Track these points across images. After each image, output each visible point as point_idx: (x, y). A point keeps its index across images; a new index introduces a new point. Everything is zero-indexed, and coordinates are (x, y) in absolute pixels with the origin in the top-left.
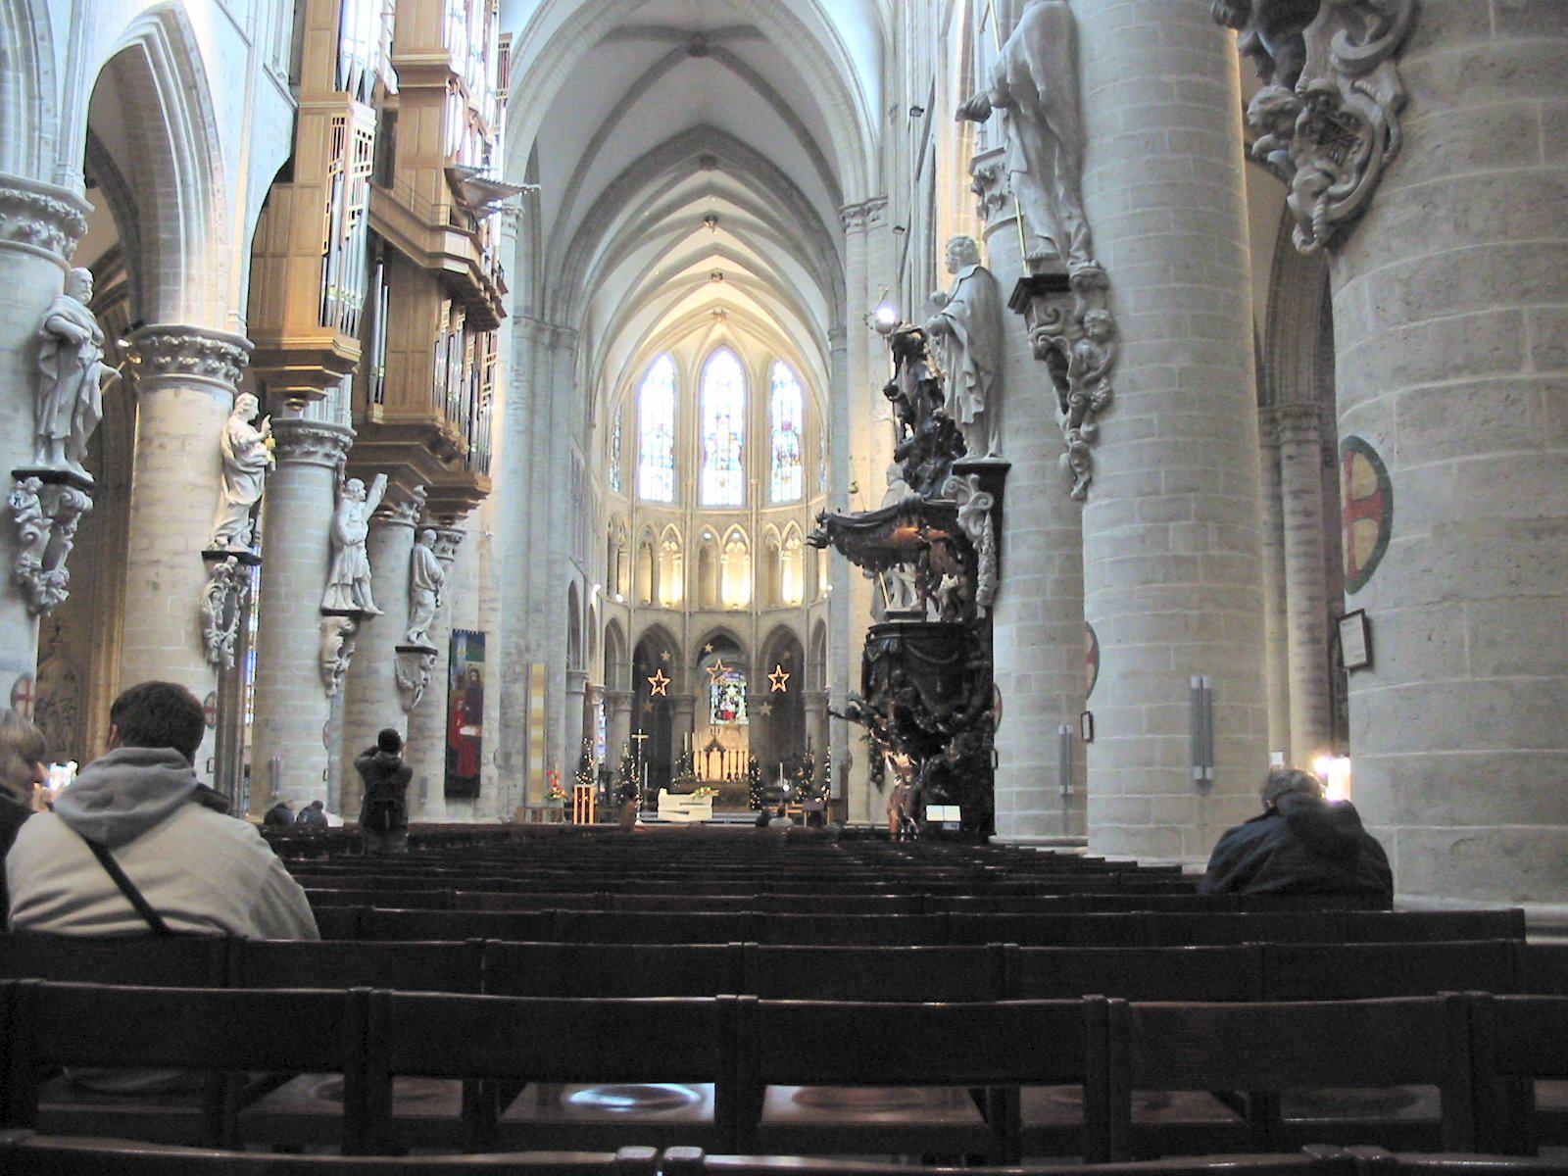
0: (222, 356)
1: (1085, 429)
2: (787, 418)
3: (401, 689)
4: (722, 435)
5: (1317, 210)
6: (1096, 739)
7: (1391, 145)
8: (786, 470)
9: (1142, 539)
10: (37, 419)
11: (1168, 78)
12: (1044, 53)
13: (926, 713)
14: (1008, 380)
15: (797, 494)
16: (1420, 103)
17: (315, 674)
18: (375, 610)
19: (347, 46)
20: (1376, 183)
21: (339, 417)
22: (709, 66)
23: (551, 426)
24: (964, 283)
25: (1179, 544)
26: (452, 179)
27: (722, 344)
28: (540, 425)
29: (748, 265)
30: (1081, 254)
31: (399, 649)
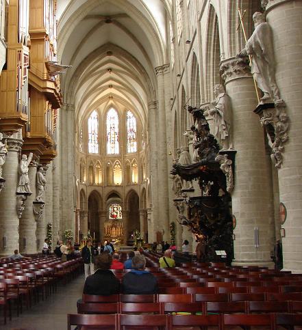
1: (280, 147)
2: (132, 128)
3: (35, 214)
4: (112, 132)
6: (286, 236)
8: (132, 143)
9: (300, 179)
12: (263, 39)
13: (209, 223)
14: (235, 127)
15: (135, 151)
19: (21, 30)
21: (19, 136)
22: (112, 26)
23: (67, 133)
26: (47, 65)
27: (112, 106)
28: (64, 133)
29: (120, 83)
30: (277, 97)
31: (34, 203)
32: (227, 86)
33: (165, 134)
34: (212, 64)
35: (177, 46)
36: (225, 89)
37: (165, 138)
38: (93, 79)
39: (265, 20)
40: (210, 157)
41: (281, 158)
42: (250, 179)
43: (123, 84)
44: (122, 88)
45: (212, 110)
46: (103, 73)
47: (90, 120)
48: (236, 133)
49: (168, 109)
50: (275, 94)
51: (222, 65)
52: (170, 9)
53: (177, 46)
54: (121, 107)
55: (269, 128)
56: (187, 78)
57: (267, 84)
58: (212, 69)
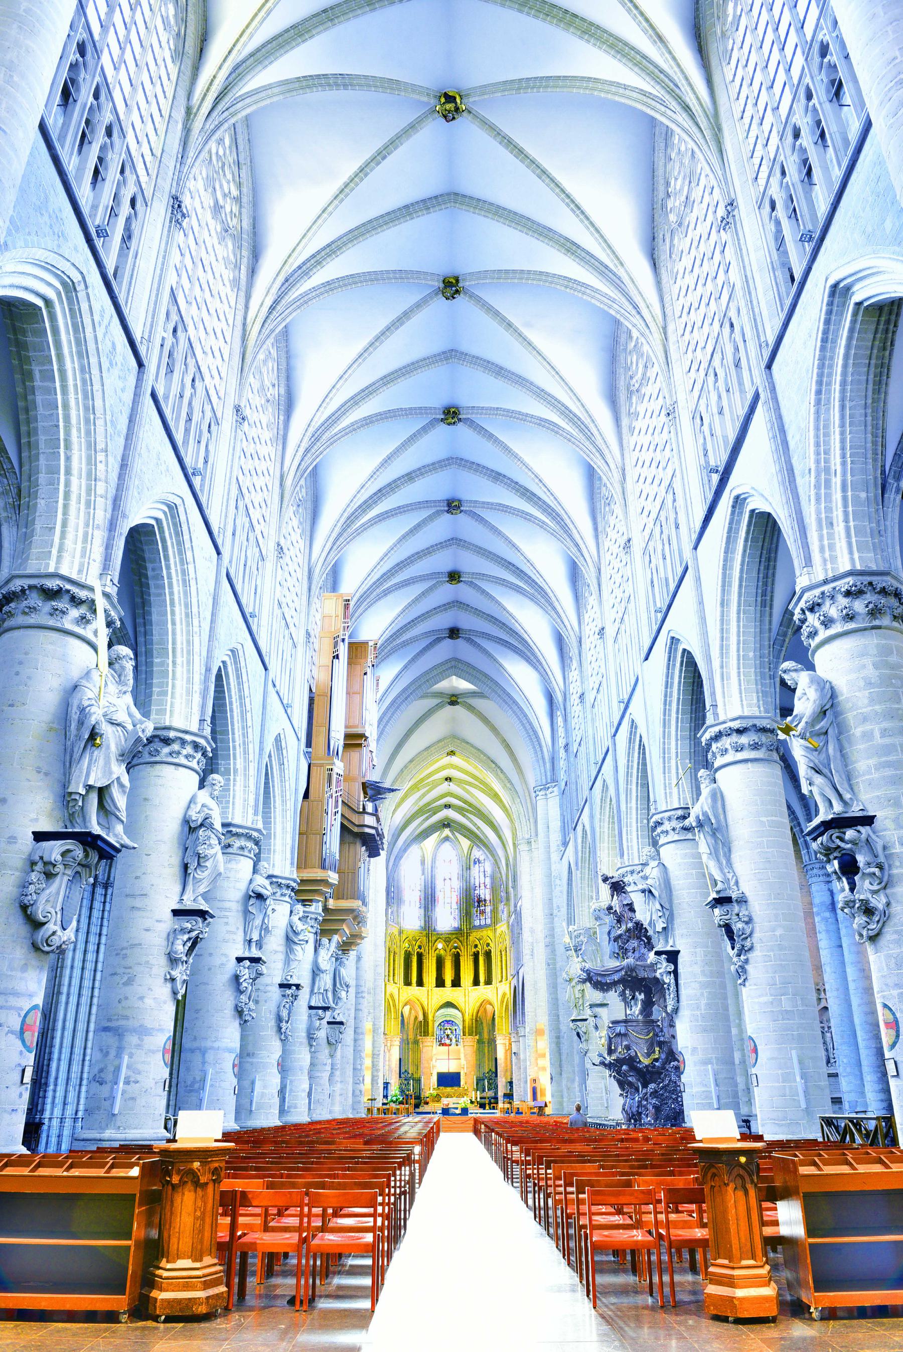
0: (288, 887)
1: (742, 957)
3: (329, 1043)
5: (865, 933)
7: (886, 916)
10: (245, 933)
11: (764, 819)
12: (714, 807)
16: (893, 904)
17: (305, 1041)
19: (332, 734)
24: (656, 870)
25: (786, 1004)
26: (365, 786)
27: (447, 839)
31: (329, 1023)
32: (662, 850)
33: (550, 899)
35: (572, 759)
36: (659, 854)
37: (551, 908)
38: (417, 795)
40: (637, 955)
41: (745, 971)
42: (702, 994)
43: (470, 805)
44: (467, 811)
45: (640, 887)
46: (435, 785)
48: (677, 922)
49: (555, 857)
50: (732, 883)
51: (653, 820)
52: (559, 697)
53: (572, 759)
57: (721, 870)
58: (634, 812)
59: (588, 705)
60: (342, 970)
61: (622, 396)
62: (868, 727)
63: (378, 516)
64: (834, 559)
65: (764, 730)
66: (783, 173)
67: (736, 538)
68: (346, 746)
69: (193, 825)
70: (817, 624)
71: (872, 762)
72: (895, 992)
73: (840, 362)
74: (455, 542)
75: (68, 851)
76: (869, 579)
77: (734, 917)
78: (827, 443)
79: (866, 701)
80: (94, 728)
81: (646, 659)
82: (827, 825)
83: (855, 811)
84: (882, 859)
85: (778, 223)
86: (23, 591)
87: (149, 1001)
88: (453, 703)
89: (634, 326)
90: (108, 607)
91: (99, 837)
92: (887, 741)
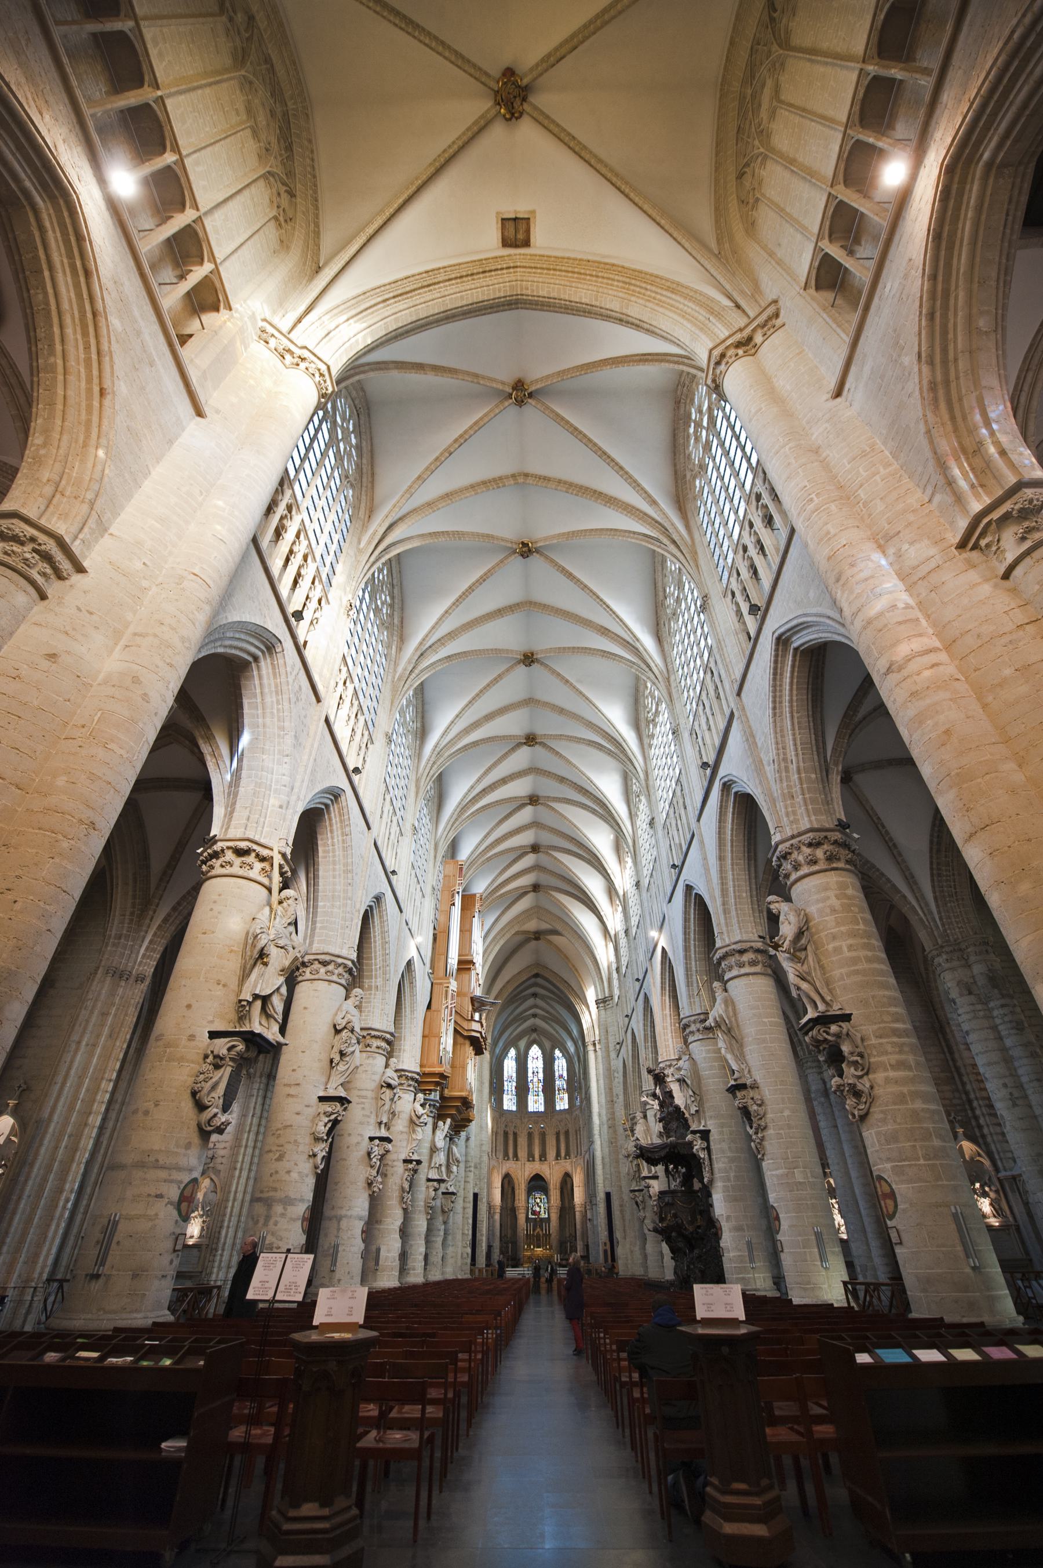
0: (412, 1079)
1: (760, 1135)
3: (443, 1212)
4: (535, 1079)
5: (856, 1113)
10: (377, 1116)
11: (766, 1020)
12: (726, 1011)
15: (567, 1107)
16: (876, 1088)
18: (445, 1177)
19: (449, 960)
20: (870, 1106)
29: (547, 1012)
31: (443, 1193)
33: (611, 1089)
34: (667, 1012)
37: (612, 1096)
39: (726, 990)
42: (731, 1168)
45: (677, 1076)
46: (525, 998)
47: (506, 1061)
48: (707, 1105)
49: (613, 1055)
50: (746, 1072)
54: (547, 1045)
55: (745, 1112)
56: (638, 1022)
59: (631, 938)
60: (454, 1148)
61: (643, 725)
62: (837, 944)
63: (483, 807)
64: (796, 821)
65: (758, 951)
66: (739, 574)
67: (726, 812)
68: (459, 970)
69: (338, 1028)
70: (789, 867)
71: (844, 971)
72: (888, 1166)
73: (788, 688)
74: (535, 824)
75: (234, 1046)
76: (824, 834)
77: (750, 1102)
78: (783, 742)
79: (834, 924)
80: (263, 949)
81: (670, 901)
82: (815, 1022)
83: (835, 1010)
84: (861, 1049)
85: (737, 604)
86: (223, 851)
87: (294, 1175)
88: (537, 939)
89: (648, 678)
90: (282, 862)
91: (260, 1035)
92: (854, 954)
